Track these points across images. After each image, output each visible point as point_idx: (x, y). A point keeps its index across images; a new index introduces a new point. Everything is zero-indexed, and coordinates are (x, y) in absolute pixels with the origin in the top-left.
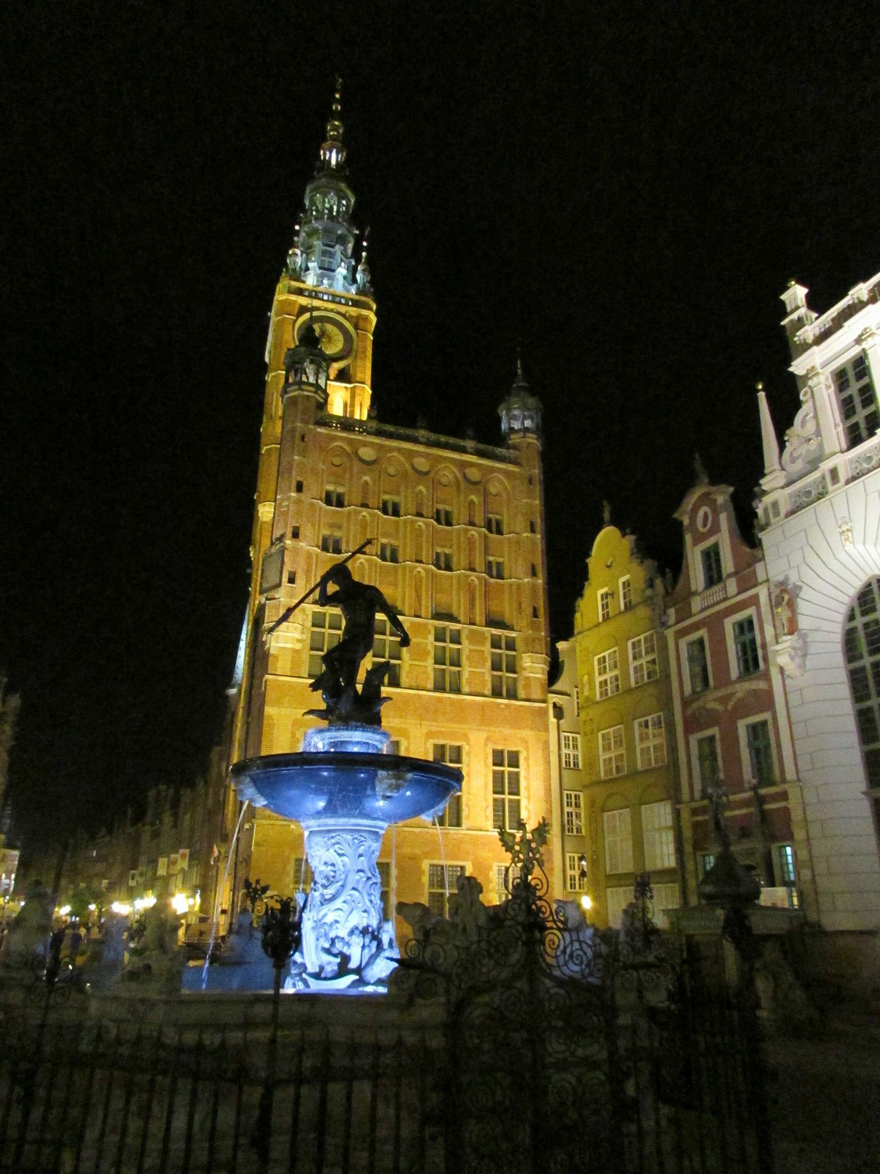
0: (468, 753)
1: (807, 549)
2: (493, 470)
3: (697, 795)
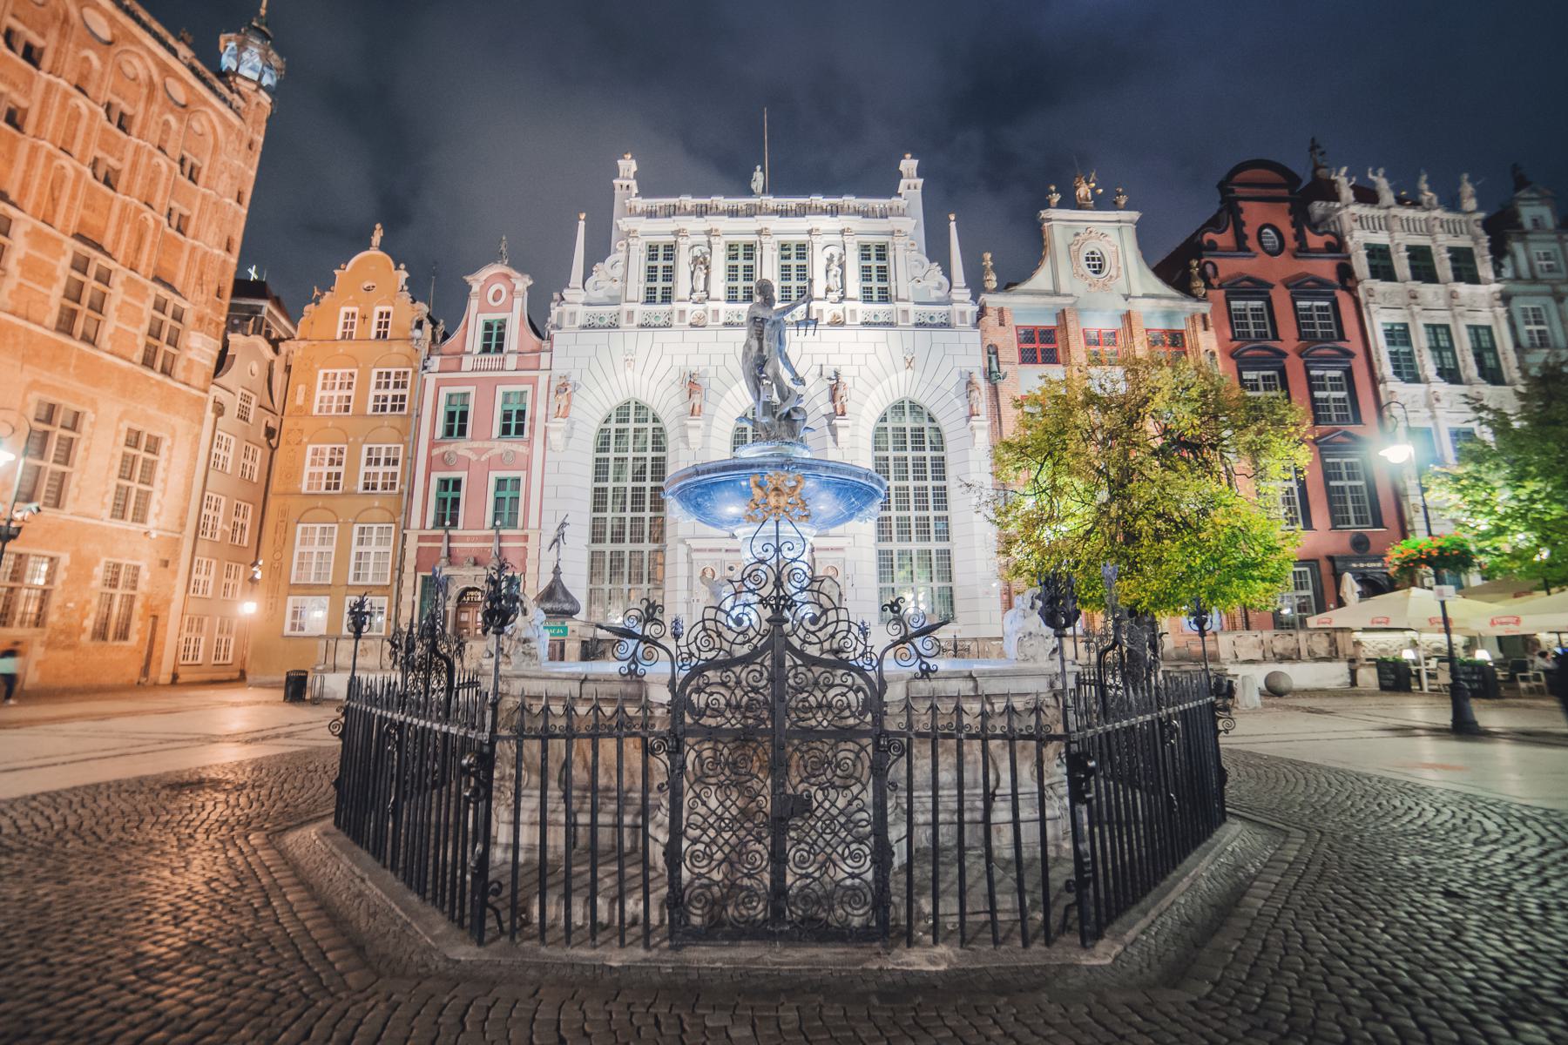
0: (93, 425)
1: (593, 360)
2: (206, 102)
3: (429, 524)
